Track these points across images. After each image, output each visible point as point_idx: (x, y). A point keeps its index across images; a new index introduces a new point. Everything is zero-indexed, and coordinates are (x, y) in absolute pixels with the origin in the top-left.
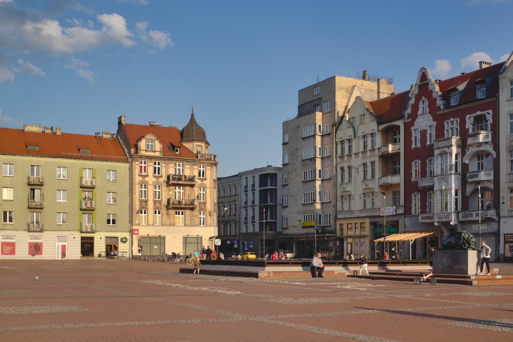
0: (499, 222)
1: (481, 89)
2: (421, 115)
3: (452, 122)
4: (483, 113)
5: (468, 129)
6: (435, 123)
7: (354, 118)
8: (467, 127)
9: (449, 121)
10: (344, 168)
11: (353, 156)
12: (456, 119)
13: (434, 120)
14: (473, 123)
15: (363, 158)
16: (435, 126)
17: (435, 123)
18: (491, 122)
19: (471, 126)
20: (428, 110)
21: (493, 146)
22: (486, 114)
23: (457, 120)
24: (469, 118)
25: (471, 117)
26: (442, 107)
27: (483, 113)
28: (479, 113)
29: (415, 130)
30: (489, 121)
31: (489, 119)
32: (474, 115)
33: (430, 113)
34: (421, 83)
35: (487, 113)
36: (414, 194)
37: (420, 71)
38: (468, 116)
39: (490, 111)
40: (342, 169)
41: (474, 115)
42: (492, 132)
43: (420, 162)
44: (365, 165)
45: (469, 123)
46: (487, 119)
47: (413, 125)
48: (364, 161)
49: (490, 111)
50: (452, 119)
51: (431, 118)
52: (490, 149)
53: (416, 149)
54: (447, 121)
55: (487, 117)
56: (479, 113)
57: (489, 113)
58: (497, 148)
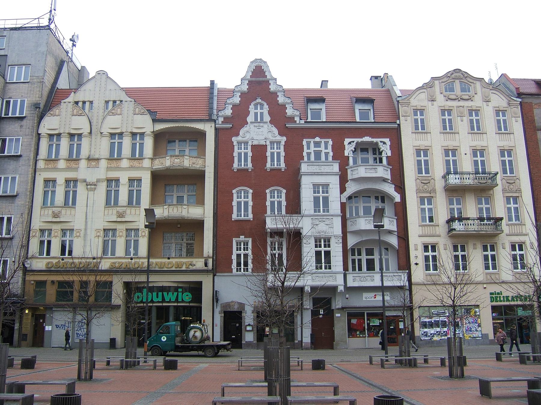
0: (410, 290)
1: (372, 110)
2: (251, 123)
3: (317, 144)
4: (375, 140)
5: (348, 157)
6: (284, 139)
7: (87, 104)
8: (346, 154)
9: (312, 141)
10: (56, 181)
11: (83, 163)
12: (326, 140)
13: (281, 134)
14: (354, 149)
15: (108, 169)
16: (283, 143)
17: (284, 139)
18: (389, 154)
19: (351, 155)
20: (267, 118)
21: (393, 186)
22: (379, 143)
23: (326, 144)
24: (350, 143)
25: (353, 142)
26: (297, 119)
27: (375, 140)
28: (367, 139)
29: (239, 143)
30: (383, 153)
31: (385, 149)
32: (360, 140)
33: (271, 122)
34: (254, 79)
35: (381, 142)
36: (238, 239)
37: (252, 62)
38: (347, 141)
39: (387, 141)
40: (50, 182)
41: (360, 140)
42: (391, 167)
43: (251, 191)
44: (111, 182)
45: (350, 149)
46: (381, 150)
47: (237, 135)
48: (113, 175)
49: (387, 141)
50: (317, 139)
51: (276, 131)
52: (390, 189)
53: (243, 171)
54: (309, 140)
55: (381, 146)
56: (367, 139)
57: (384, 143)
58: (401, 188)
